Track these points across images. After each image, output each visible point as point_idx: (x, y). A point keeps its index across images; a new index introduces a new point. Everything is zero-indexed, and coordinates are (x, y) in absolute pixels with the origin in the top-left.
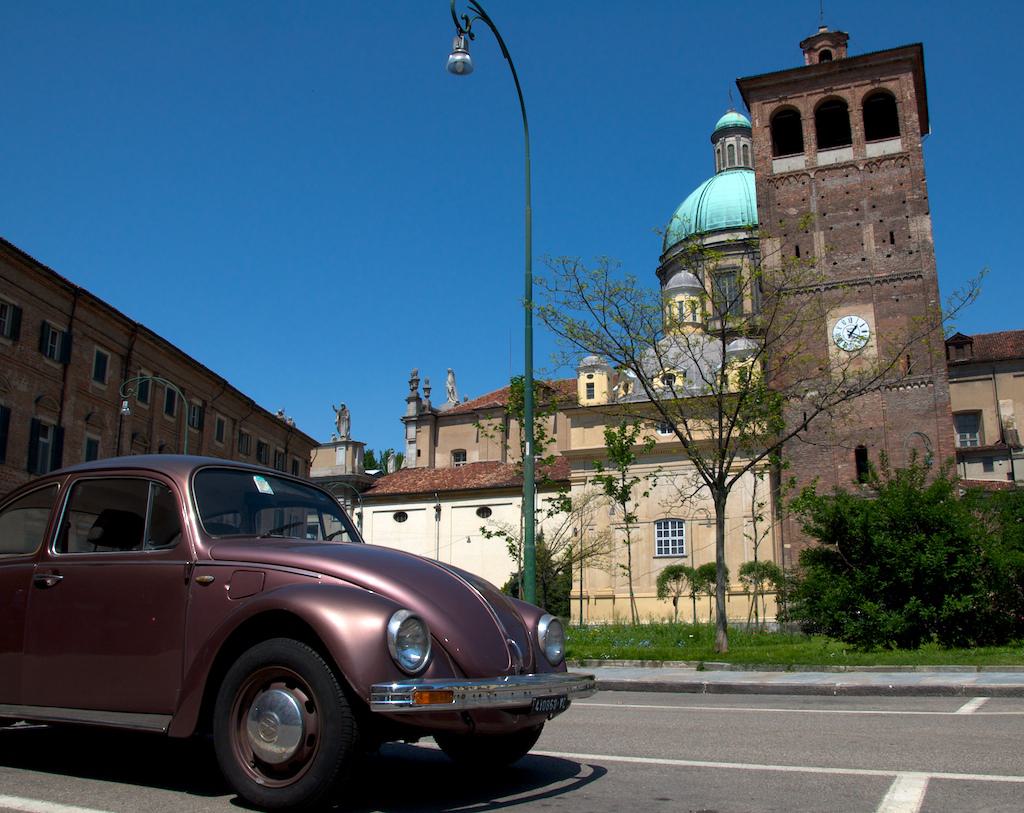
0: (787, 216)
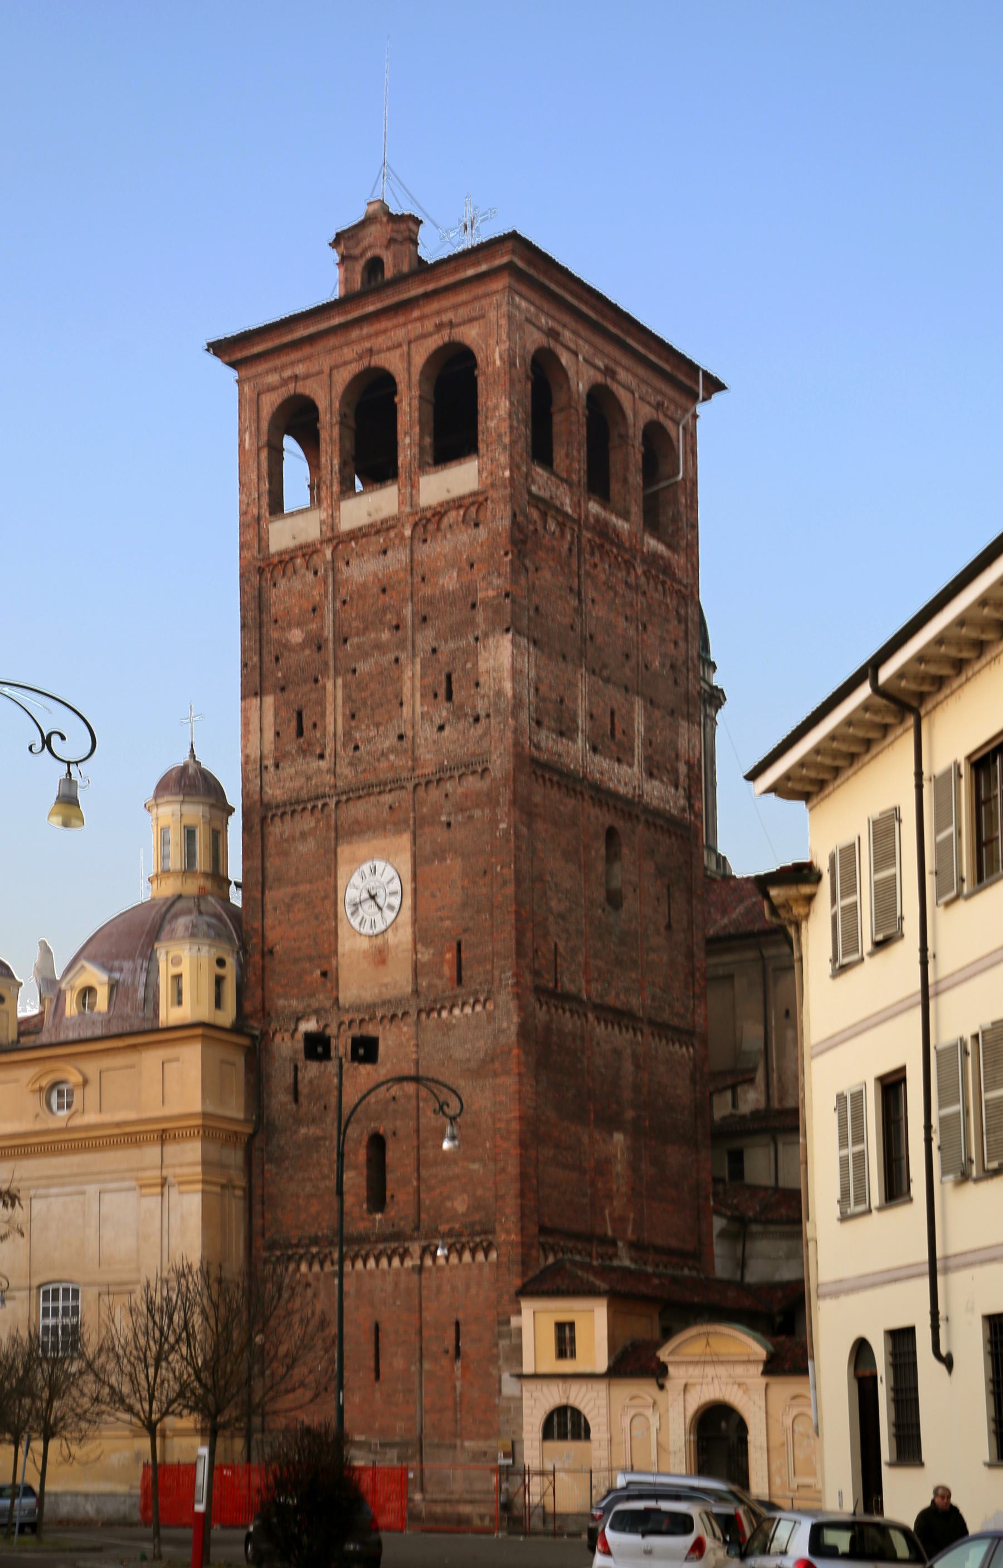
0: (286, 646)
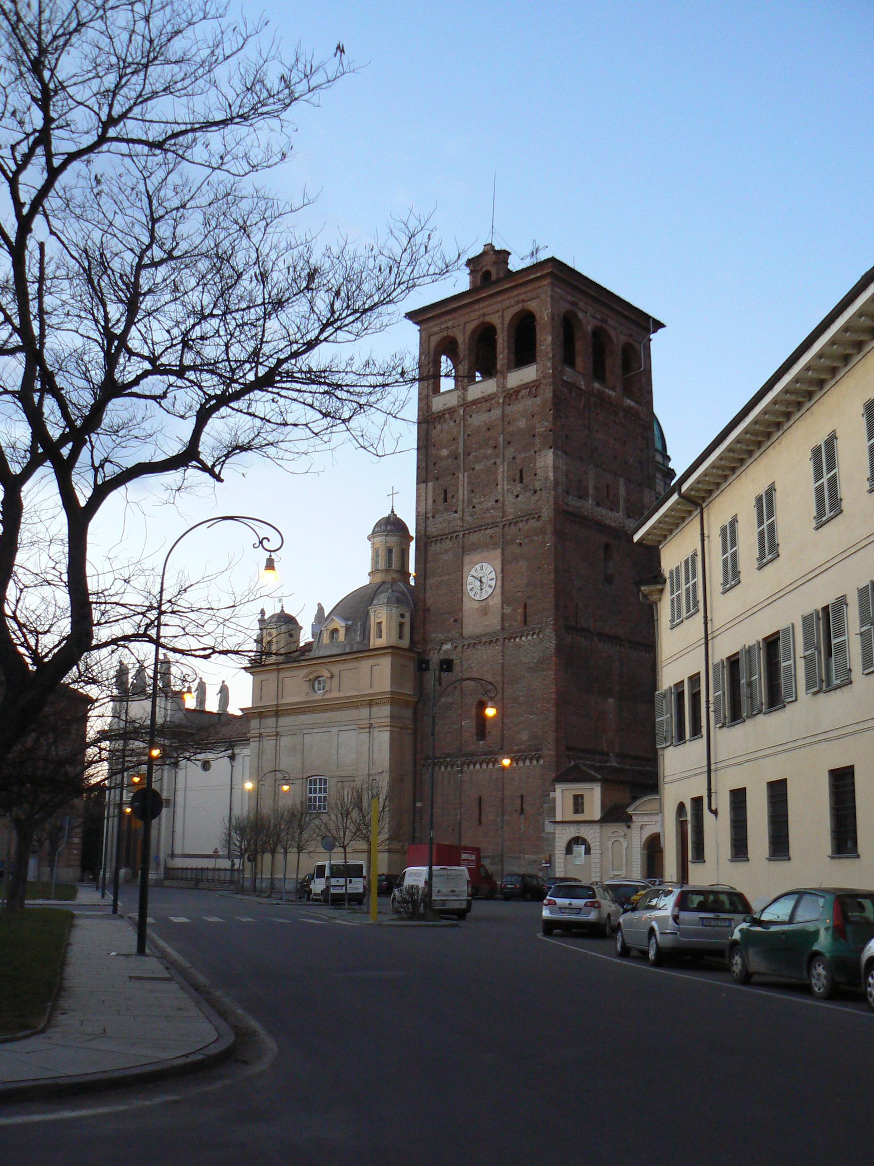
0: (440, 458)
